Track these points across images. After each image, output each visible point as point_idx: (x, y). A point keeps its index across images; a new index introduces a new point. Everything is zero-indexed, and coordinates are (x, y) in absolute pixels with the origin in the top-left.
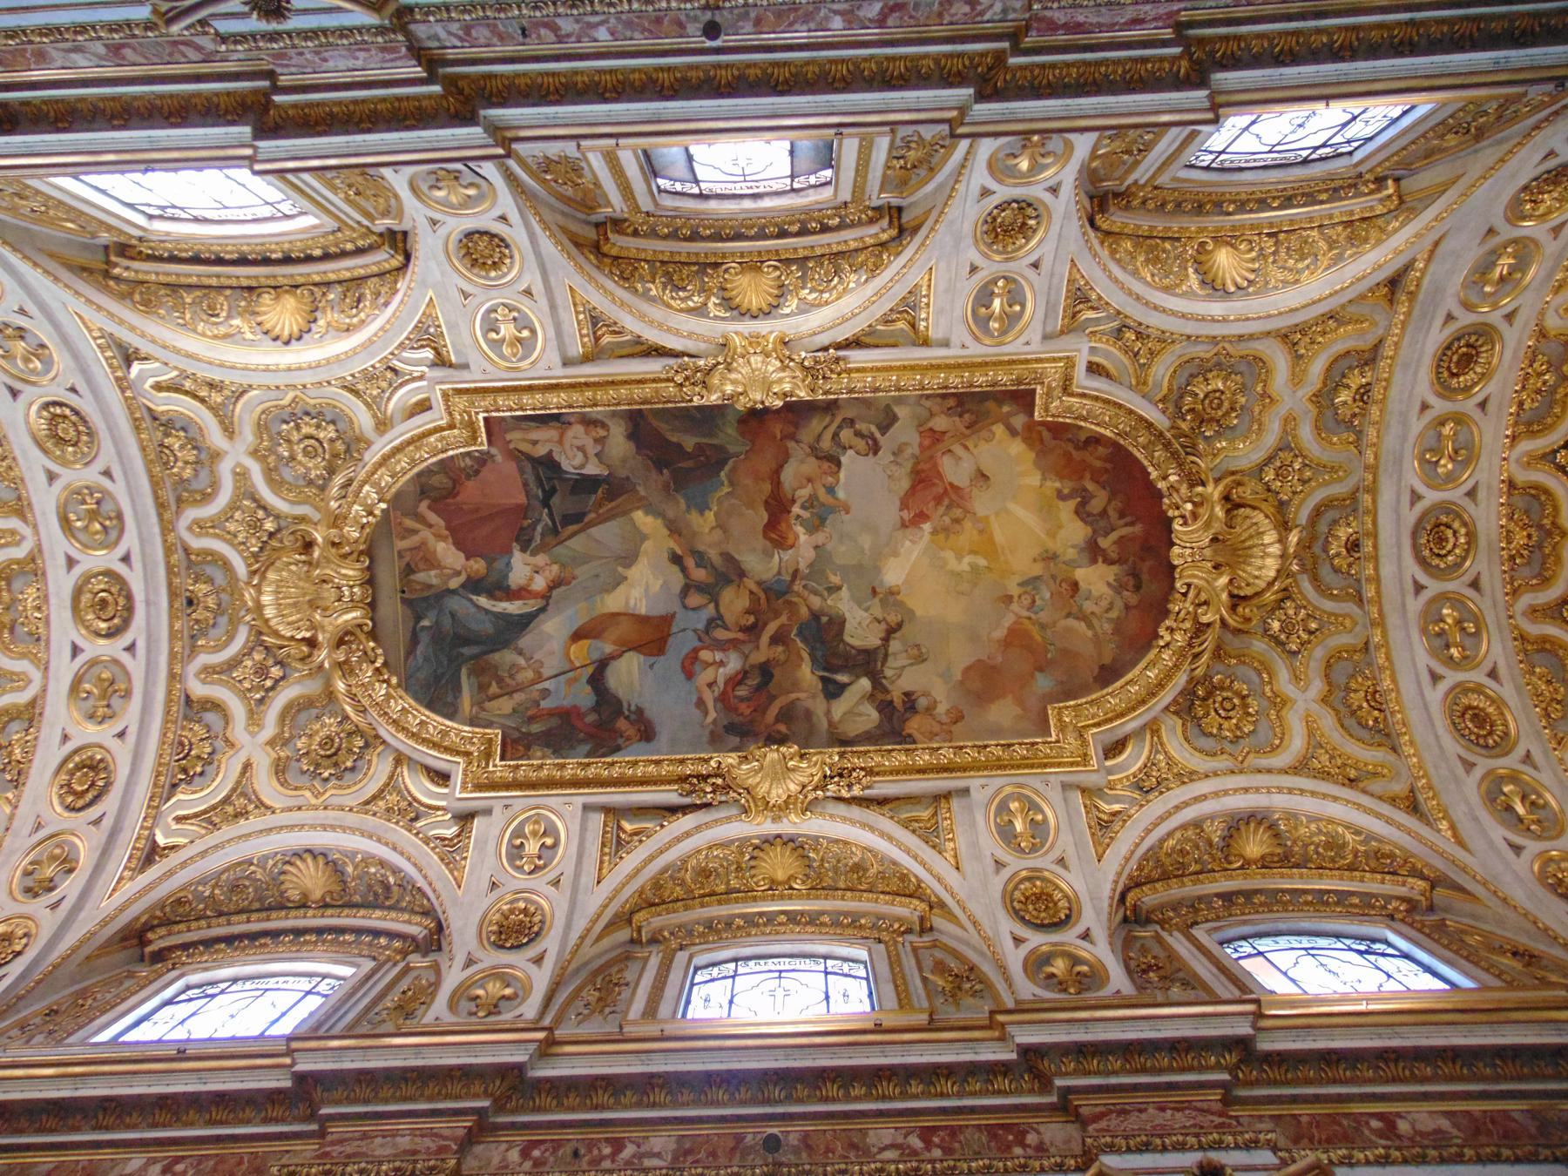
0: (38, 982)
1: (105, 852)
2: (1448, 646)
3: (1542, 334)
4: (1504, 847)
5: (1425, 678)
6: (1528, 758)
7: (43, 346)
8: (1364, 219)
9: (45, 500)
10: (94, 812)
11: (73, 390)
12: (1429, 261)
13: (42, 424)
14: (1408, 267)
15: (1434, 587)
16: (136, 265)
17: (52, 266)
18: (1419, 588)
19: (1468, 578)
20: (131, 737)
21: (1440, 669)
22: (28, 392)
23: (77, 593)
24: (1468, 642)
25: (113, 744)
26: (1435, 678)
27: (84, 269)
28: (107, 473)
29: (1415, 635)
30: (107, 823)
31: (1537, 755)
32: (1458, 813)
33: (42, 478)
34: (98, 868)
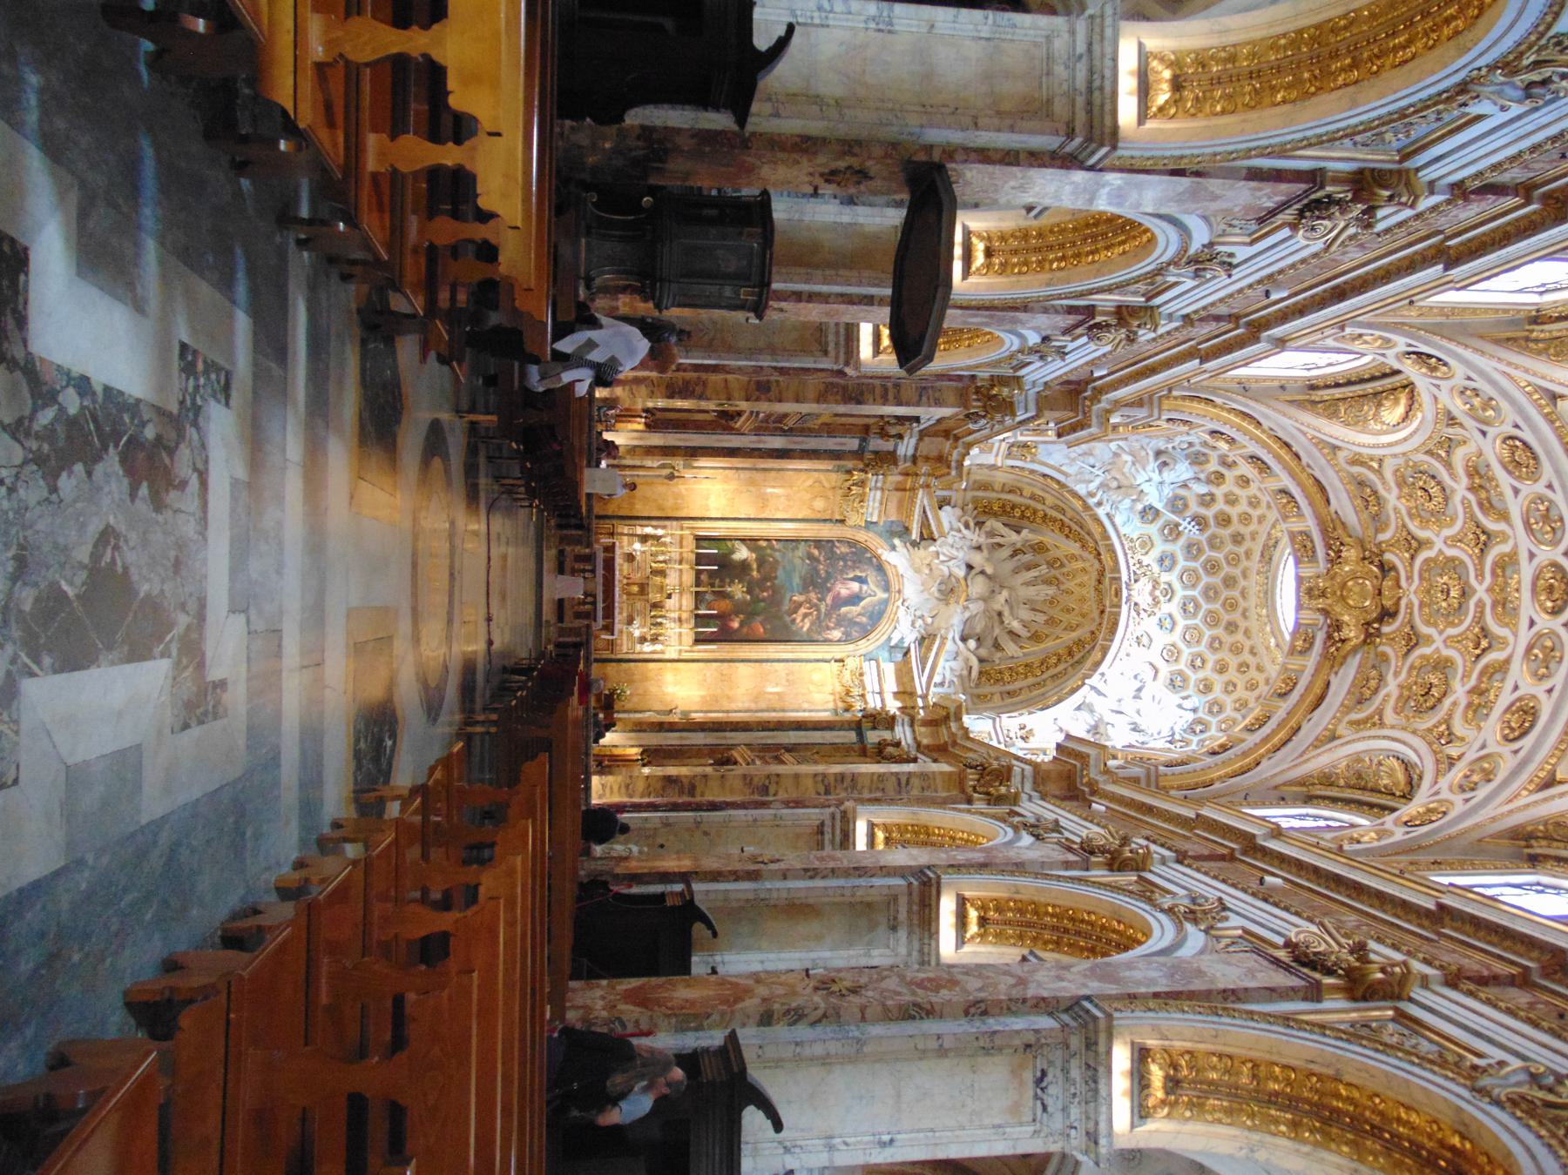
0: (1437, 843)
1: (1515, 773)
7: (1491, 399)
9: (1515, 509)
10: (1516, 746)
11: (1517, 426)
13: (1506, 453)
16: (1546, 327)
17: (1479, 344)
20: (1555, 694)
22: (1491, 431)
23: (1536, 578)
25: (1543, 696)
27: (1508, 339)
28: (1550, 486)
30: (1522, 754)
33: (1509, 493)
34: (1506, 783)
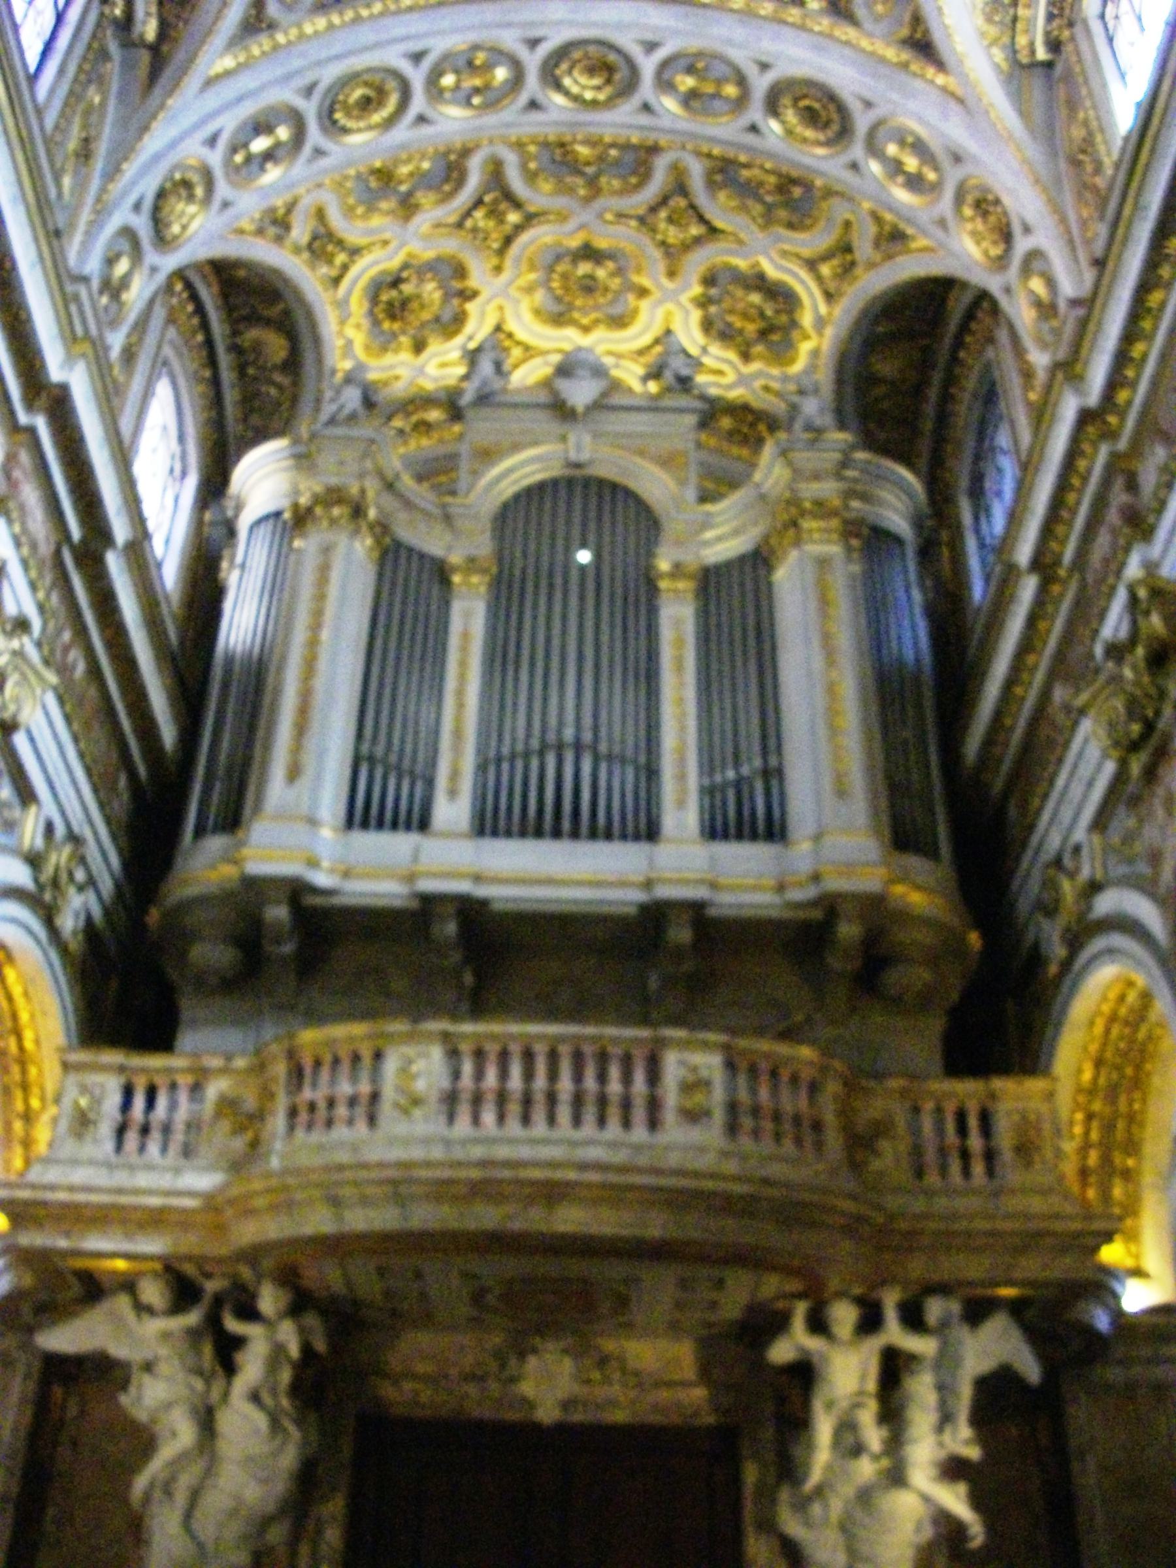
2: (457, 71)
3: (829, 193)
4: (210, 128)
5: (415, 46)
6: (319, 152)
8: (1015, 19)
12: (944, 90)
14: (941, 66)
15: (532, 61)
18: (534, 43)
19: (540, 98)
21: (427, 63)
24: (461, 95)
26: (417, 57)
29: (472, 37)
31: (324, 162)
32: (246, 82)
